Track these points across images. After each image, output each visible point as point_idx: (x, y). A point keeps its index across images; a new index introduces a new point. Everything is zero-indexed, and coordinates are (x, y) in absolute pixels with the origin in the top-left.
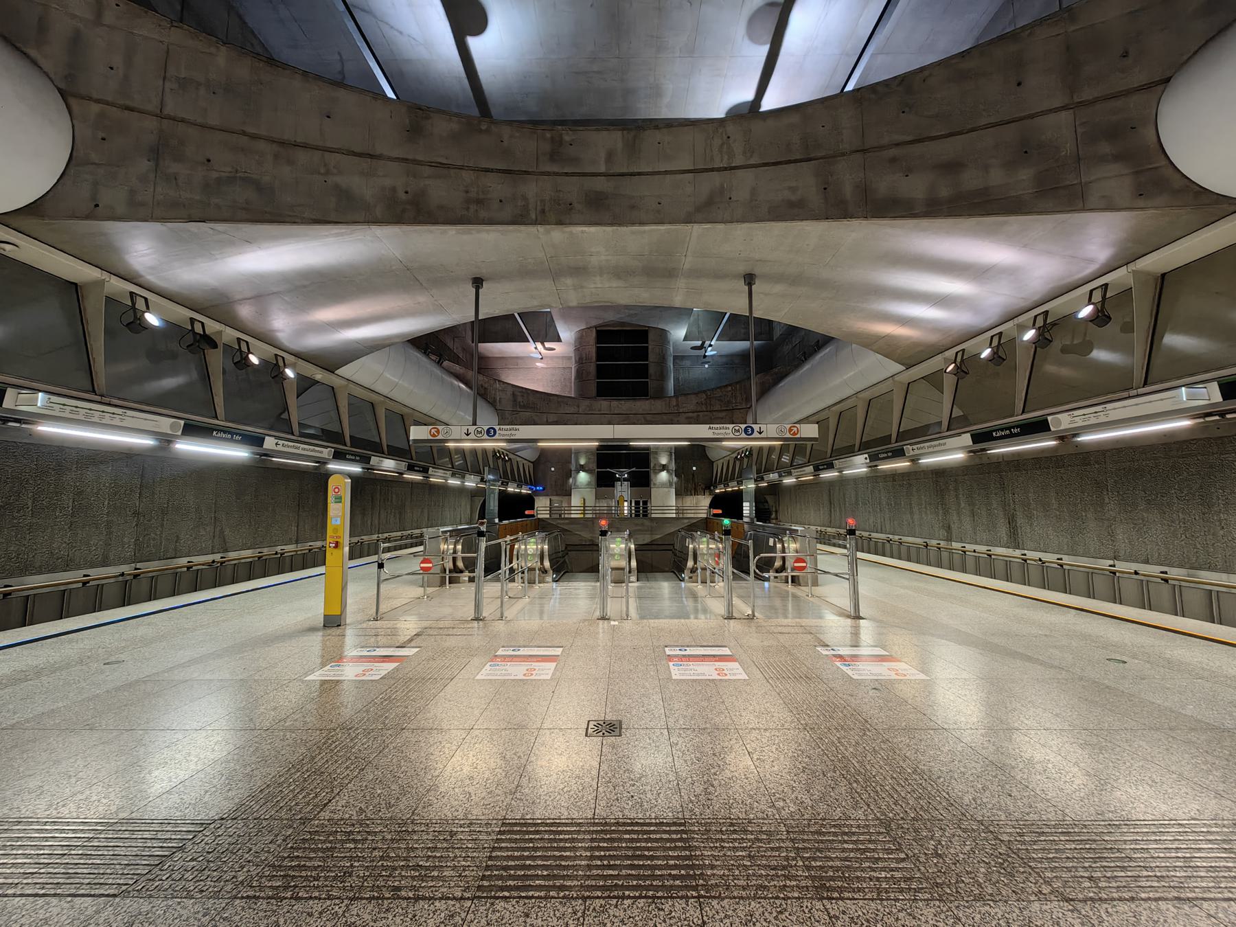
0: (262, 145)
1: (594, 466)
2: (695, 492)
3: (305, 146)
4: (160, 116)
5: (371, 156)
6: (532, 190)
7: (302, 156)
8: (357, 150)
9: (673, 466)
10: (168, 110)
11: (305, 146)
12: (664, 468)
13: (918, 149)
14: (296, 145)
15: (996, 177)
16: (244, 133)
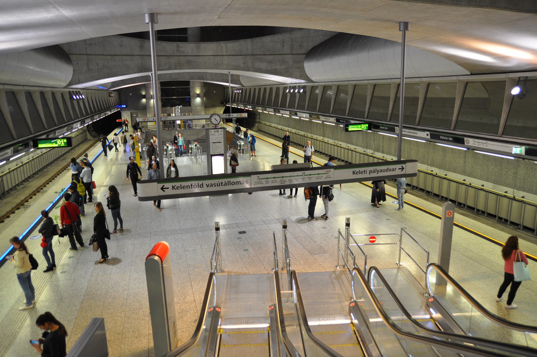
0: (108, 57)
1: (159, 95)
2: (214, 106)
3: (117, 55)
4: (87, 55)
5: (132, 55)
6: (173, 60)
7: (116, 57)
8: (129, 54)
9: (202, 95)
10: (88, 53)
11: (117, 55)
12: (198, 96)
13: (264, 57)
14: (115, 55)
15: (278, 67)
16: (103, 55)
